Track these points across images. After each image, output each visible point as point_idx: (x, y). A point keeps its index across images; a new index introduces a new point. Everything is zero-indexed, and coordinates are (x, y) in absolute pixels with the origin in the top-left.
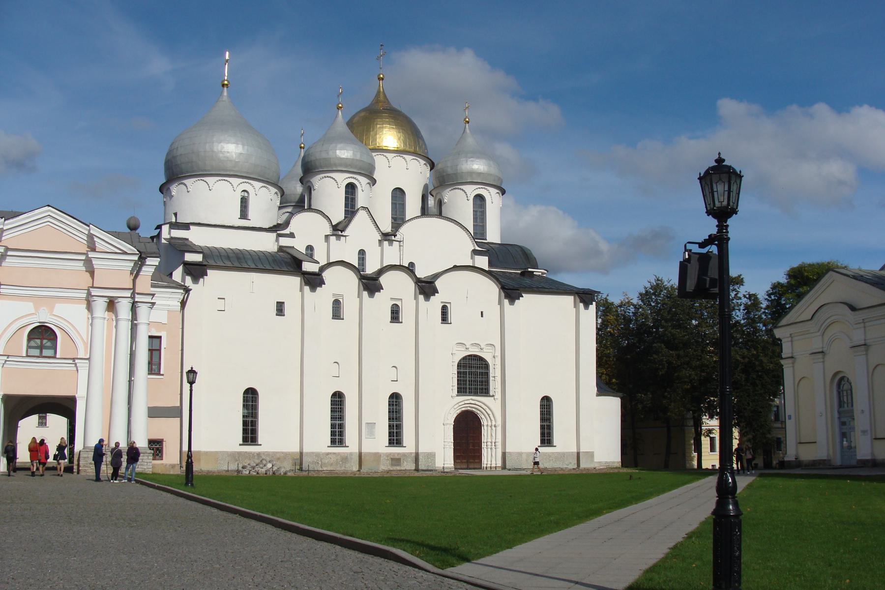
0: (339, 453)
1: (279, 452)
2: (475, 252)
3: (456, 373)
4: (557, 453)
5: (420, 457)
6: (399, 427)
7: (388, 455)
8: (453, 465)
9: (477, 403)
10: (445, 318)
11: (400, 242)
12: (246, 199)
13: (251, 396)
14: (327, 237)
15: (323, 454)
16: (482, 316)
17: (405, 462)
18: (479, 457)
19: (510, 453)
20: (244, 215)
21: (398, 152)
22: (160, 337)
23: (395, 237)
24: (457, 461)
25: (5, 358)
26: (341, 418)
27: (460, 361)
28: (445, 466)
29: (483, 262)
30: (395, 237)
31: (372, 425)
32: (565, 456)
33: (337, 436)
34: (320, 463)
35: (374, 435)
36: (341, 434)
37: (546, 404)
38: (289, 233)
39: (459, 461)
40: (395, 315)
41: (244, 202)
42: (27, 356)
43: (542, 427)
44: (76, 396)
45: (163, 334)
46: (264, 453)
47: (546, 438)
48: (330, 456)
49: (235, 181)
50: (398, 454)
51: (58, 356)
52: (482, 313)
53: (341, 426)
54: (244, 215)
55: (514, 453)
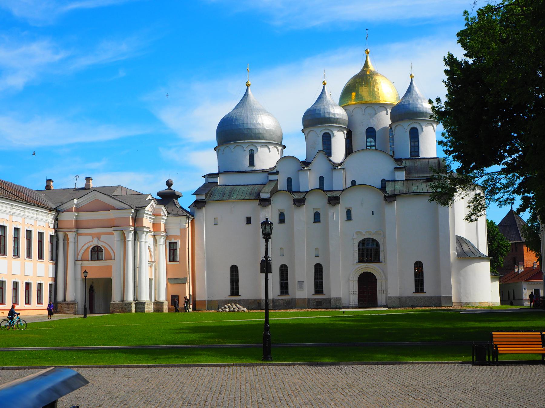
0: (285, 299)
1: (250, 300)
2: (396, 169)
3: (357, 249)
4: (426, 297)
5: (332, 301)
6: (322, 283)
7: (314, 299)
8: (358, 305)
10: (349, 217)
11: (343, 169)
12: (252, 154)
15: (276, 299)
16: (373, 214)
17: (325, 304)
18: (376, 299)
19: (391, 297)
20: (252, 163)
22: (176, 243)
23: (337, 167)
24: (361, 302)
25: (81, 262)
28: (350, 305)
29: (401, 175)
30: (337, 167)
31: (301, 283)
32: (433, 299)
34: (271, 305)
35: (303, 288)
36: (287, 288)
37: (419, 265)
38: (276, 172)
39: (362, 302)
40: (317, 218)
42: (92, 260)
44: (111, 277)
45: (179, 242)
46: (242, 300)
47: (419, 286)
48: (279, 301)
49: (245, 146)
50: (320, 299)
51: (104, 259)
52: (373, 212)
55: (393, 297)
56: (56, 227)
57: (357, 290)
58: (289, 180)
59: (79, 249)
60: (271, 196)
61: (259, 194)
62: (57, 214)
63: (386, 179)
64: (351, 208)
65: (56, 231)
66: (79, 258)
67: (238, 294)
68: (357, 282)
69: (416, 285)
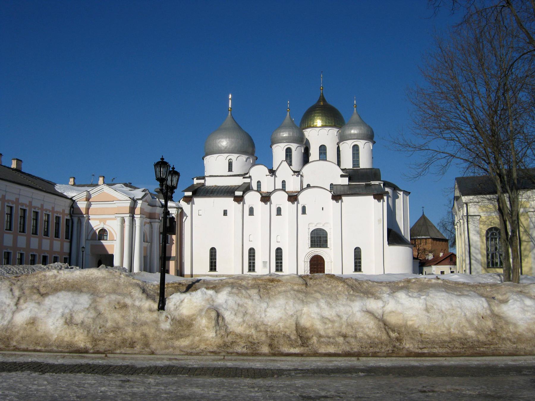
9: (321, 251)
13: (213, 252)
14: (267, 175)
16: (323, 209)
20: (230, 169)
21: (323, 126)
26: (254, 259)
27: (312, 231)
29: (345, 181)
31: (264, 263)
33: (252, 268)
36: (254, 266)
41: (230, 164)
43: (355, 263)
49: (226, 155)
51: (108, 240)
52: (323, 208)
53: (254, 263)
54: (230, 169)
56: (72, 213)
57: (309, 269)
58: (259, 182)
59: (89, 232)
60: (243, 194)
61: (234, 193)
62: (72, 202)
63: (334, 184)
64: (306, 204)
65: (71, 216)
66: (90, 238)
67: (216, 270)
68: (309, 263)
69: (356, 266)
